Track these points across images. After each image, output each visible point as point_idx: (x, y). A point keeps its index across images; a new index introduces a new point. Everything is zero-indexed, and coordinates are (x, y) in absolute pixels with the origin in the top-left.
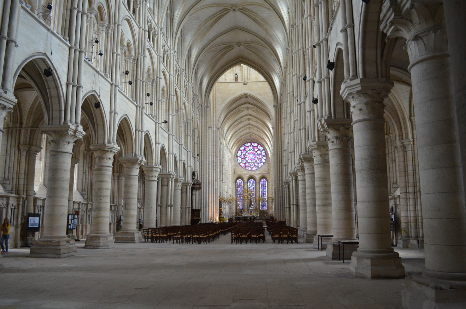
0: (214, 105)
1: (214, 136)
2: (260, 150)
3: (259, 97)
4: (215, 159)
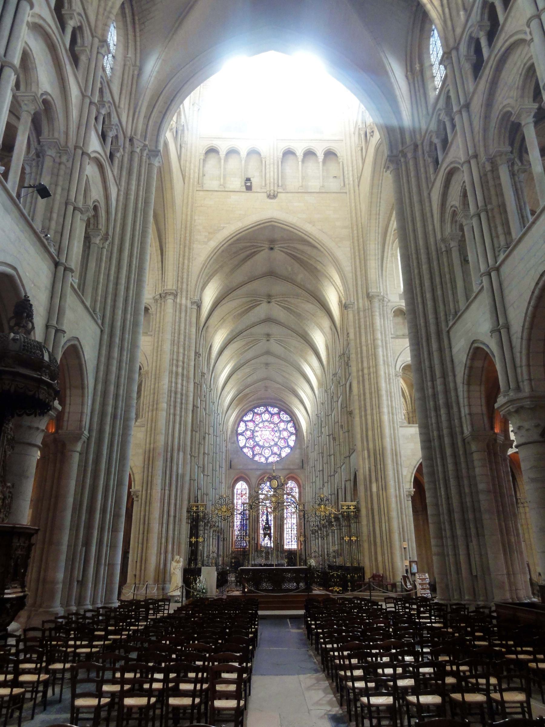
0: (185, 239)
1: (183, 320)
2: (283, 421)
3: (309, 228)
4: (182, 385)
